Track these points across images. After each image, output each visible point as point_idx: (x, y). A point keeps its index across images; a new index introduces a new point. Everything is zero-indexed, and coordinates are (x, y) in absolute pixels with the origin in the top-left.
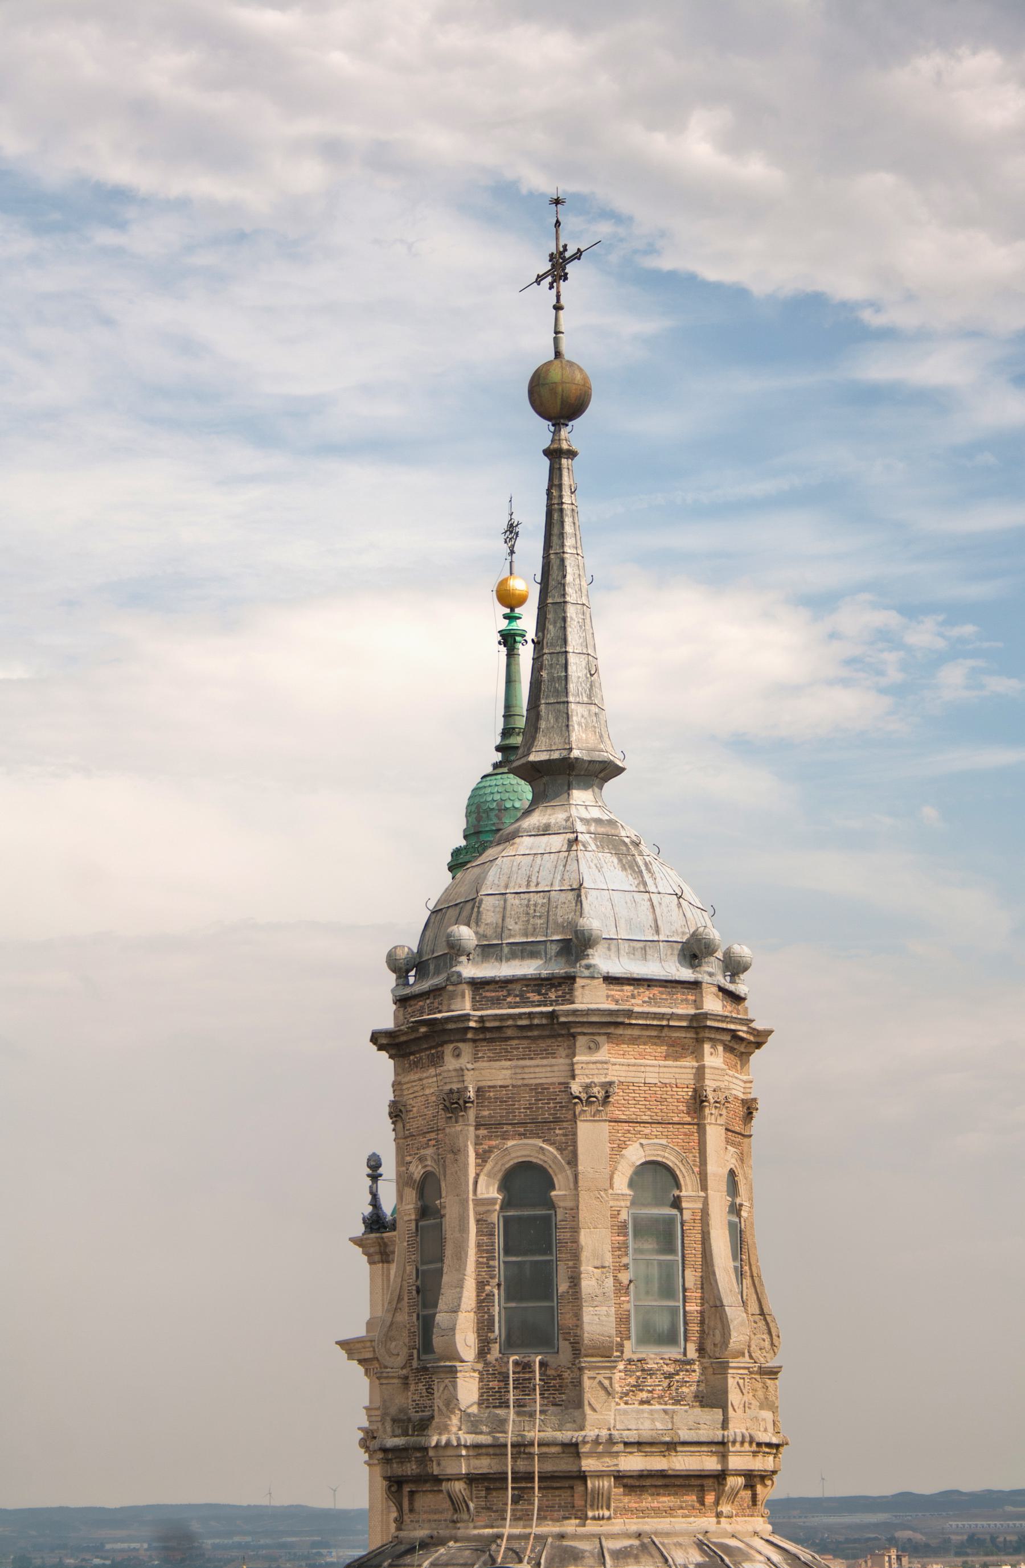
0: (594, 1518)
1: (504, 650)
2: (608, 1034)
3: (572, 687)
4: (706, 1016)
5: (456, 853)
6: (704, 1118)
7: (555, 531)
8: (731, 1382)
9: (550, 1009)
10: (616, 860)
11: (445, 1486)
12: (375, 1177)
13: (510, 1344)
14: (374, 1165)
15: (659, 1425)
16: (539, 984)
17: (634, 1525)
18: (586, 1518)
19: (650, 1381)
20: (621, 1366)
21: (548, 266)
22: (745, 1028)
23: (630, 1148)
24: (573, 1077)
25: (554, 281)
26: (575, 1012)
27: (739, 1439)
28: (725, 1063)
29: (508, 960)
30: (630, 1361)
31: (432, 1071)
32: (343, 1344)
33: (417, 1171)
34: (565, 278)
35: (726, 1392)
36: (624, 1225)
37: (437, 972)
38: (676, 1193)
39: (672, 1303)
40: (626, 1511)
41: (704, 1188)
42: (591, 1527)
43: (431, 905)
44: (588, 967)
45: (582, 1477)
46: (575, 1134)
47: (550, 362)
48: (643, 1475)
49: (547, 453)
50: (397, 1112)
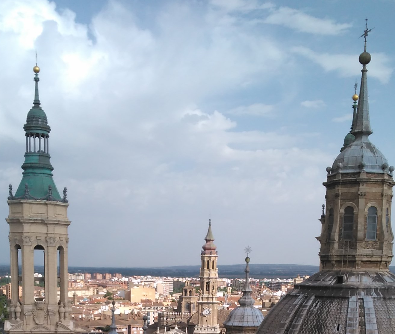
0: (357, 268)
1: (353, 109)
2: (366, 183)
3: (364, 117)
4: (384, 180)
5: (342, 148)
6: (383, 198)
7: (363, 86)
8: (384, 245)
9: (355, 178)
10: (370, 150)
11: (331, 262)
12: (323, 208)
13: (345, 238)
14: (323, 206)
15: (370, 253)
16: (354, 174)
17: (364, 269)
18: (356, 268)
19: (369, 245)
20: (364, 242)
21: (364, 33)
22: (392, 182)
23: (369, 204)
24: (359, 191)
25: (365, 36)
26: (360, 179)
27: (385, 255)
28: (388, 188)
29: (348, 169)
30: (366, 241)
31: (333, 190)
32: (316, 238)
33: (329, 208)
34: (367, 35)
35: (383, 247)
36: (366, 218)
37: (335, 172)
38: (376, 212)
39: (374, 232)
40: (362, 267)
41: (382, 211)
42: (357, 270)
43: (335, 159)
44: (363, 171)
45: (356, 261)
46: (358, 201)
47: (363, 53)
48: (366, 261)
49: (362, 71)
50: (326, 197)
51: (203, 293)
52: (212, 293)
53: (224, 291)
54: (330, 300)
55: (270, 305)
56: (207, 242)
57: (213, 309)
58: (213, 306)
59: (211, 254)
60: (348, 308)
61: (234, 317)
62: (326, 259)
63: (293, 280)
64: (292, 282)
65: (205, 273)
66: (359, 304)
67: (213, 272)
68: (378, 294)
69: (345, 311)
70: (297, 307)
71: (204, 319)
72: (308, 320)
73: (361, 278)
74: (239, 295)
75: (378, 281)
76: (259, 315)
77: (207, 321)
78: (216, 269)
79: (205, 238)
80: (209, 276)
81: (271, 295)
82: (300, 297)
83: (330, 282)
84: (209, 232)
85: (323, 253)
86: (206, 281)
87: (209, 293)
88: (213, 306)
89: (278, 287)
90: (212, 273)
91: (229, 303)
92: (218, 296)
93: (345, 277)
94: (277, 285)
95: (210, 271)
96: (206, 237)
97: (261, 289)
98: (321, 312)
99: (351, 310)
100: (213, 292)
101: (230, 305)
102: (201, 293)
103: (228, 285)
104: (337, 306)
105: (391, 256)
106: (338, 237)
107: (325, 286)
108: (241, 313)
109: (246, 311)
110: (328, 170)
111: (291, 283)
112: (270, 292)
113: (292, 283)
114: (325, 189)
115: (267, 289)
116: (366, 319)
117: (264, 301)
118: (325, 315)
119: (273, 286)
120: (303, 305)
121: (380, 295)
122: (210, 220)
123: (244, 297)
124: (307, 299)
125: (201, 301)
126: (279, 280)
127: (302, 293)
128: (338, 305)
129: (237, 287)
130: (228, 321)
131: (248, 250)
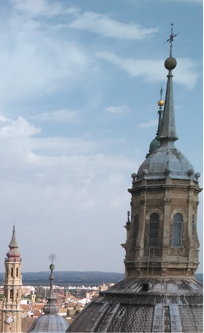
0: (163, 275)
1: (159, 115)
2: (171, 190)
3: (169, 123)
4: (190, 186)
5: (147, 155)
6: (189, 205)
7: (168, 92)
8: (190, 253)
9: (161, 185)
10: (175, 156)
11: (137, 269)
12: (129, 215)
13: (150, 245)
14: (129, 213)
15: (176, 260)
16: (159, 180)
17: (170, 277)
18: (161, 275)
19: (175, 252)
20: (170, 249)
21: (170, 38)
22: (198, 188)
23: (174, 211)
24: (165, 197)
25: (171, 41)
26: (166, 185)
27: (190, 262)
28: (194, 195)
29: (154, 176)
30: (171, 249)
31: (138, 196)
32: (122, 245)
33: (135, 214)
34: (173, 40)
35: (189, 254)
36: (172, 225)
37: (140, 178)
38: (182, 219)
39: (180, 239)
40: (168, 274)
41: (188, 218)
42: (162, 277)
43: (140, 166)
44: (169, 177)
45: (161, 269)
46: (164, 208)
47: (169, 58)
48: (172, 268)
49: (167, 76)
50: (132, 204)
51: (7, 301)
52: (16, 301)
53: (28, 299)
54: (135, 308)
55: (74, 313)
56: (11, 249)
57: (17, 317)
58: (17, 314)
59: (15, 262)
60: (153, 315)
61: (38, 325)
62: (131, 266)
63: (98, 287)
64: (96, 289)
65: (9, 281)
66: (164, 312)
67: (17, 279)
68: (183, 302)
69: (151, 319)
70: (102, 314)
71: (8, 327)
72: (113, 328)
73: (166, 286)
74: (44, 303)
75: (184, 288)
76: (64, 323)
77: (11, 328)
78: (20, 277)
79: (8, 245)
80: (13, 284)
81: (76, 302)
82: (105, 305)
83: (136, 289)
84: (13, 239)
85: (128, 260)
86: (10, 288)
87: (13, 301)
88: (17, 314)
89: (83, 295)
90: (16, 280)
91: (33, 311)
92: (22, 304)
93: (151, 284)
94: (82, 293)
95: (14, 279)
96: (10, 244)
97: (66, 297)
98: (126, 320)
99: (157, 318)
100: (17, 300)
101: (35, 313)
102: (5, 301)
103: (32, 292)
104: (142, 314)
105: (197, 263)
106: (143, 244)
107: (130, 293)
108: (45, 321)
109: (50, 319)
110: (133, 176)
111: (95, 290)
112: (75, 300)
113: (97, 290)
114: (130, 195)
115: (71, 297)
116: (172, 327)
117: (69, 308)
118: (130, 323)
119: (77, 293)
120: (108, 312)
121: (186, 303)
122: (14, 227)
123: (48, 305)
124: (112, 306)
125: (5, 309)
126: (83, 288)
127: (107, 301)
128: (144, 313)
129: (42, 294)
130: (32, 329)
131: (52, 257)
